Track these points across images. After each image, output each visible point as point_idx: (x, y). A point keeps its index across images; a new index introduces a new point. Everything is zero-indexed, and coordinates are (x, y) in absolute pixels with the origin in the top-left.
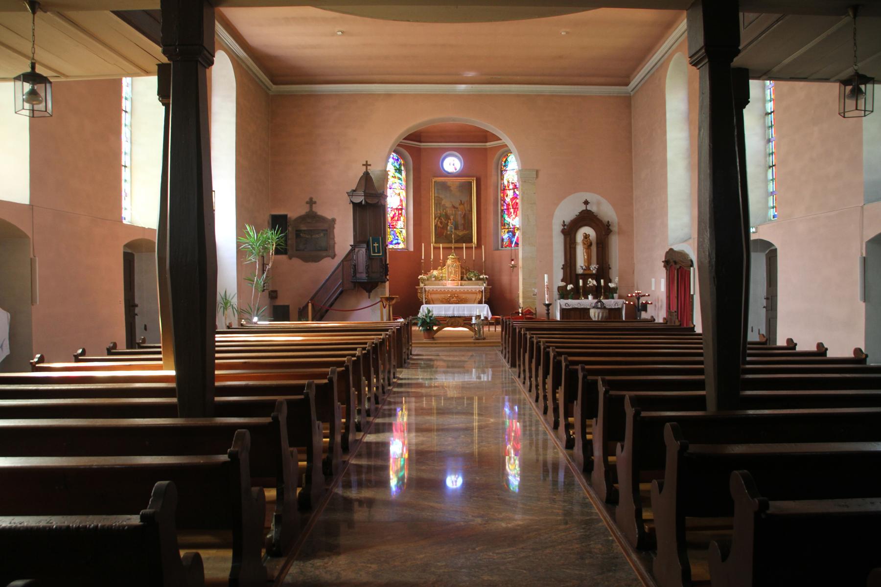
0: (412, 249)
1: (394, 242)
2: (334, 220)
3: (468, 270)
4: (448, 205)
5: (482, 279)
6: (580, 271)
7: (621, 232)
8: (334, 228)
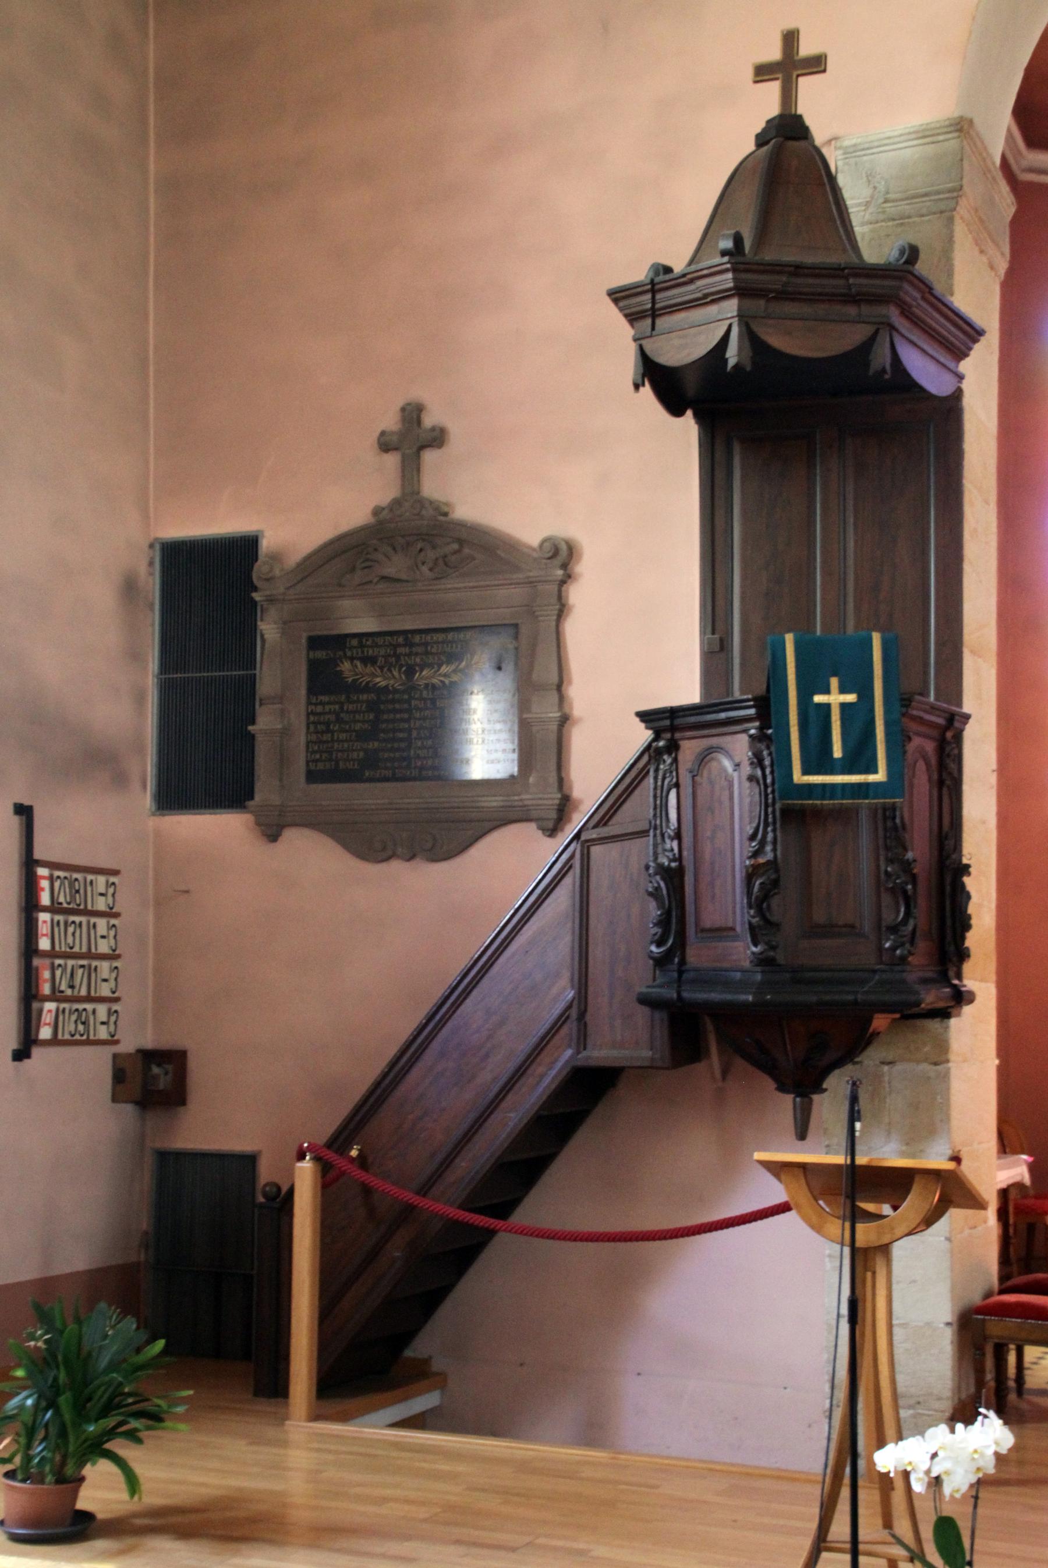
2: (562, 556)
8: (562, 610)
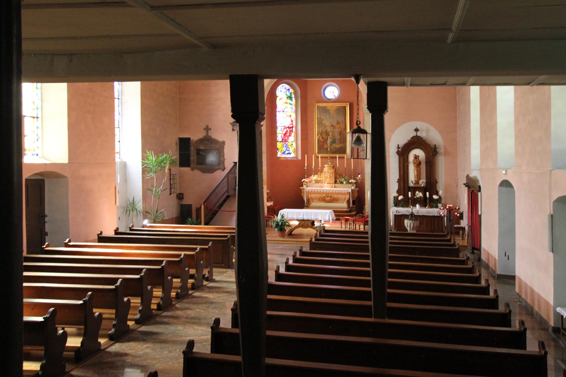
0: (300, 158)
1: (287, 152)
3: (341, 176)
4: (328, 124)
5: (351, 183)
6: (411, 185)
7: (446, 153)
8: (224, 148)
